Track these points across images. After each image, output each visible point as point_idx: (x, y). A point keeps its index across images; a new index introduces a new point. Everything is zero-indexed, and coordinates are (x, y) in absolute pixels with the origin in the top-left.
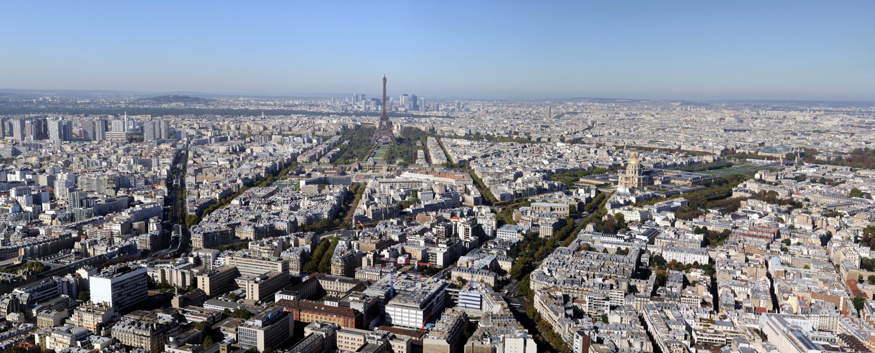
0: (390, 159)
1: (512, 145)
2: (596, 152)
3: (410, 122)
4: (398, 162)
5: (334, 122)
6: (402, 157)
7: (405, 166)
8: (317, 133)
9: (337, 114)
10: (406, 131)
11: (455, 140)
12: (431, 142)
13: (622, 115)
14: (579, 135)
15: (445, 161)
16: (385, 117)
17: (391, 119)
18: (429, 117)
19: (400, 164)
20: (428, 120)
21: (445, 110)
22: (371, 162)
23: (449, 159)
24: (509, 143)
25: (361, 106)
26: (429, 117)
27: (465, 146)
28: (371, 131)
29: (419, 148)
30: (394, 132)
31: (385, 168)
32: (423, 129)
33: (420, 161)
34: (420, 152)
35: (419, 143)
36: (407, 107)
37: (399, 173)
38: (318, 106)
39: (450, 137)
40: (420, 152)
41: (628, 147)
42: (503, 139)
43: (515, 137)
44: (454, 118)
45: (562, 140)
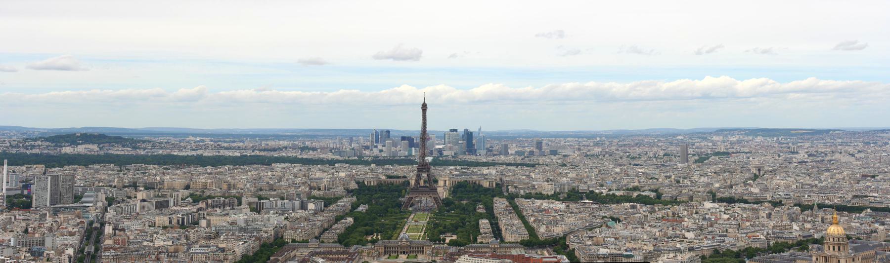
1: (633, 207)
2: (769, 216)
3: (465, 174)
4: (448, 240)
8: (315, 193)
10: (459, 188)
11: (538, 202)
12: (500, 204)
13: (802, 155)
14: (738, 190)
15: (526, 237)
16: (424, 167)
18: (494, 164)
19: (453, 243)
20: (494, 172)
21: (518, 153)
23: (531, 231)
24: (628, 205)
27: (555, 210)
29: (481, 216)
30: (439, 190)
32: (486, 184)
34: (484, 224)
35: (481, 209)
38: (314, 149)
39: (528, 196)
40: (484, 224)
41: (821, 206)
42: (616, 200)
43: (635, 194)
44: (533, 166)
45: (713, 197)
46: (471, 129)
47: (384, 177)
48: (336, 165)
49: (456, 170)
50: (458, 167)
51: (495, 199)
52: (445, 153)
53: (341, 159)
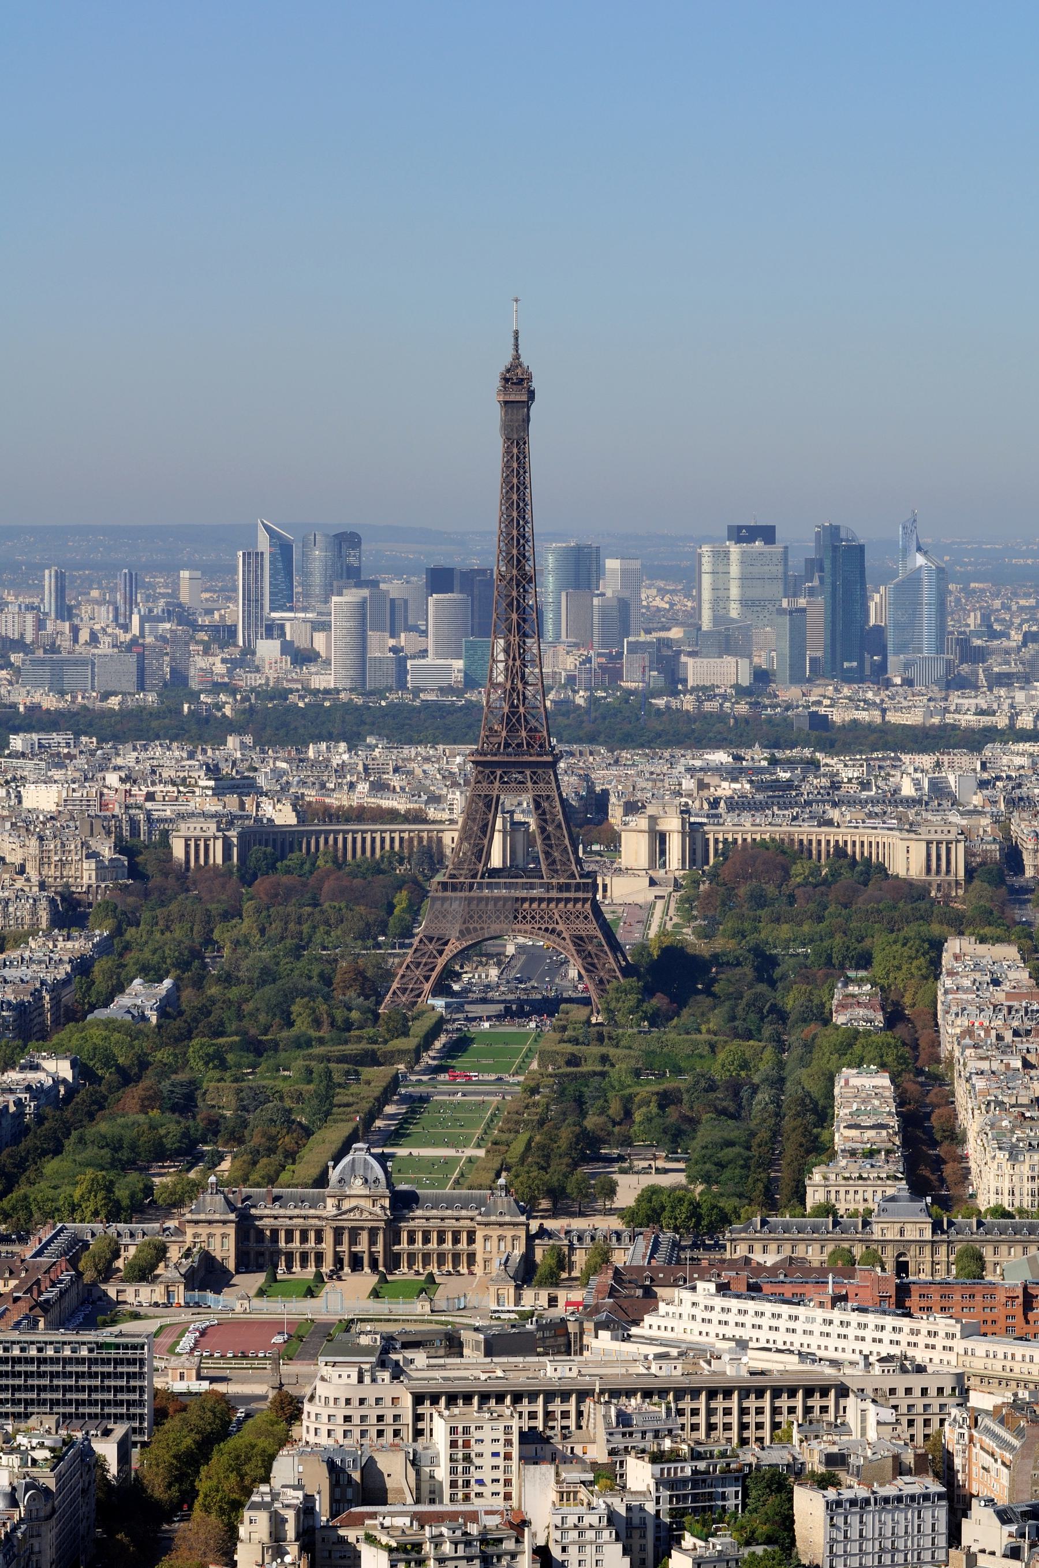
0: (558, 1164)
3: (778, 794)
4: (629, 1190)
5: (42, 798)
6: (675, 1139)
7: (691, 1236)
9: (77, 722)
17: (611, 772)
18: (975, 740)
19: (650, 1212)
22: (357, 1191)
25: (323, 647)
26: (975, 740)
28: (394, 886)
29: (851, 1049)
31: (498, 1246)
32: (906, 859)
33: (855, 1181)
34: (864, 1094)
36: (770, 650)
37: (627, 1303)
40: (864, 1094)
46: (859, 530)
47: (284, 816)
48: (17, 742)
49: (733, 774)
50: (757, 756)
51: (955, 946)
52: (696, 670)
53: (50, 702)
